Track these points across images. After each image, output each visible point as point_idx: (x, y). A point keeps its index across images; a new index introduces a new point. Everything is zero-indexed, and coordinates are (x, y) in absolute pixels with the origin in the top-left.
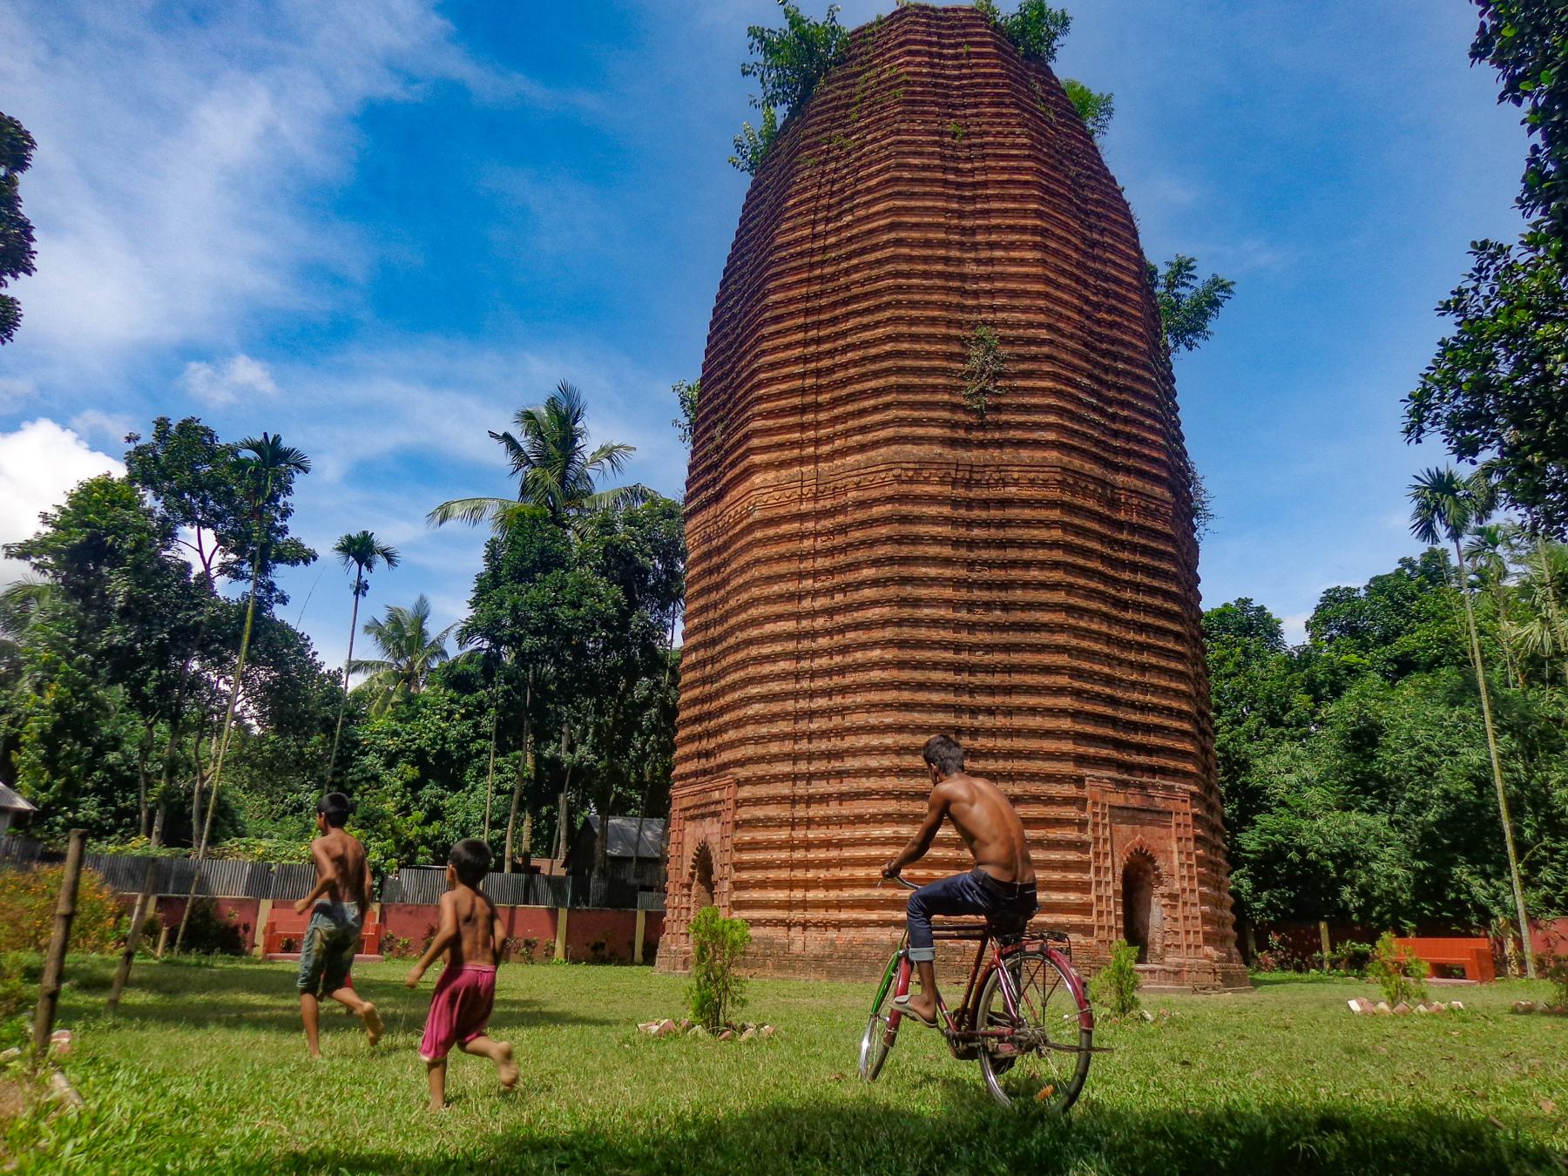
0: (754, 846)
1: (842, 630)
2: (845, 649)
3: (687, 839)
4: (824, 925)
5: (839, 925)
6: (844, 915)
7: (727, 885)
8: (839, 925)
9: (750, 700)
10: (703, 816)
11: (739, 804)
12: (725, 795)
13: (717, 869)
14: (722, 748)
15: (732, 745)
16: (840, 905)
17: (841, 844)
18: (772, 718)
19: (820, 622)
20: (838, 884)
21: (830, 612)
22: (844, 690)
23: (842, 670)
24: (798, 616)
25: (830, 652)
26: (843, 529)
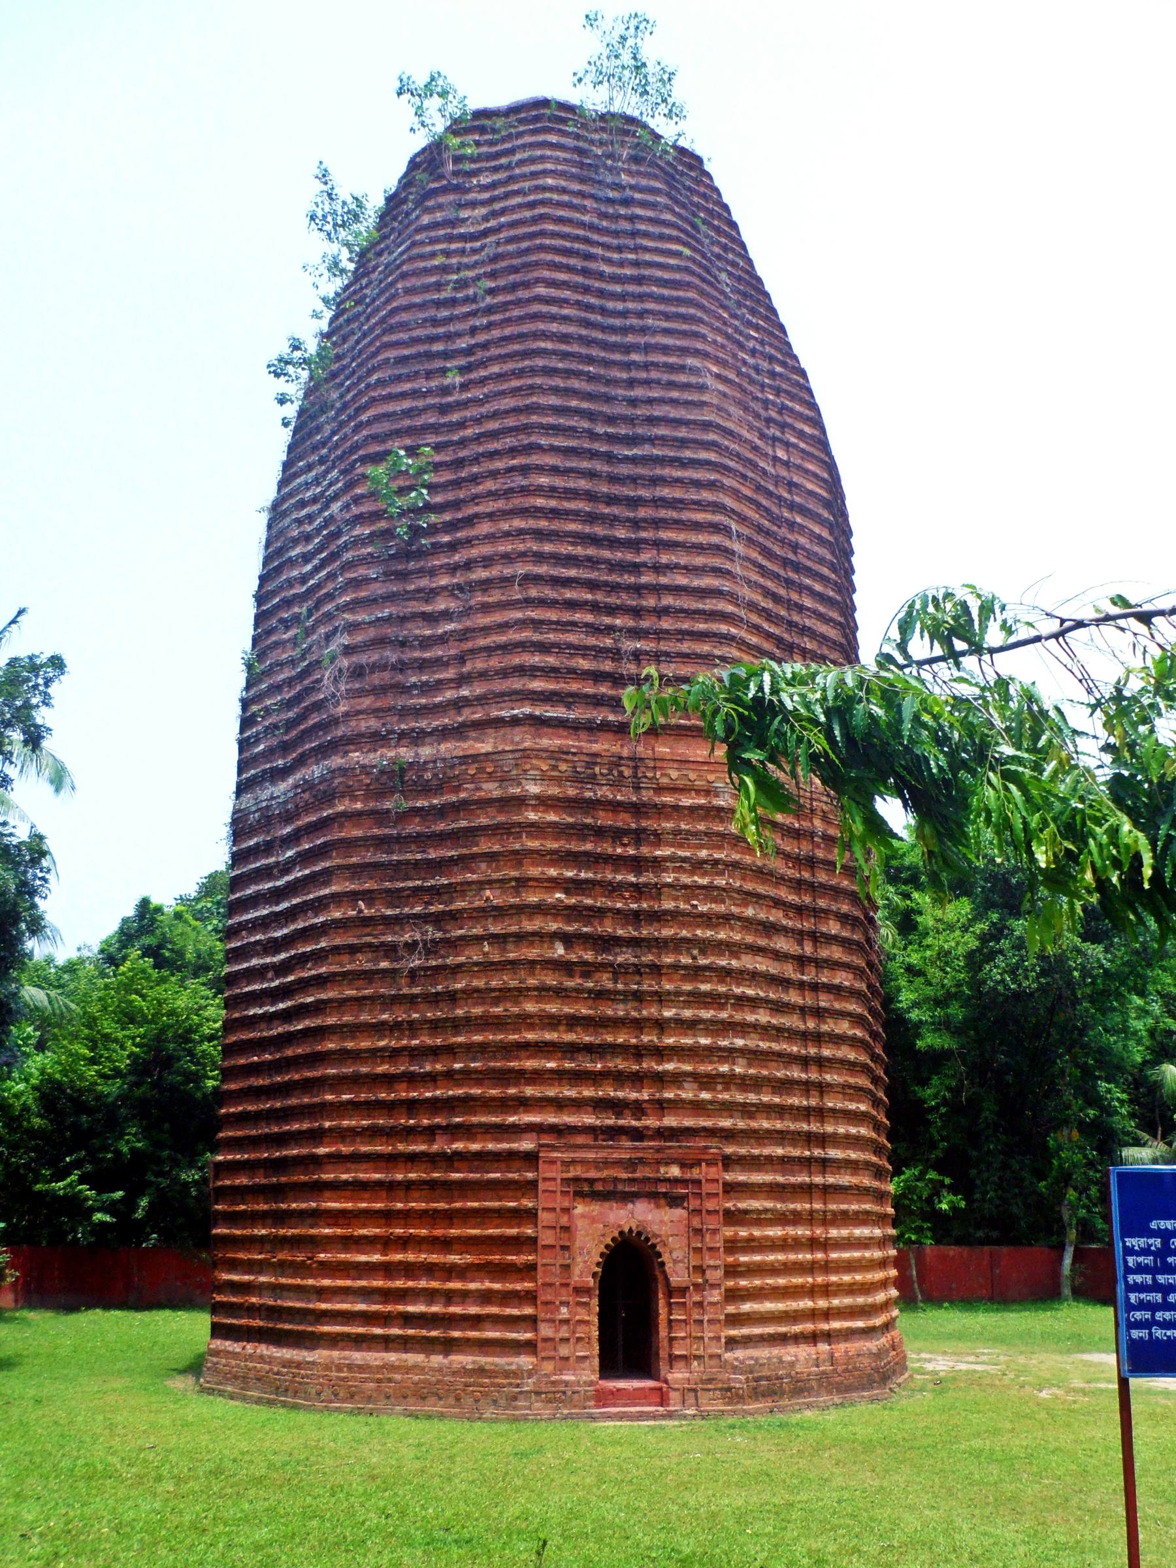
0: (751, 1245)
1: (815, 987)
2: (819, 1013)
3: (580, 1224)
4: (813, 1338)
5: (828, 1336)
6: (836, 1325)
7: (715, 1296)
8: (828, 1336)
9: (730, 1054)
10: (627, 1198)
11: (731, 1189)
12: (695, 1173)
13: (678, 1276)
14: (662, 1106)
15: (698, 1107)
16: (827, 1314)
17: (825, 1245)
18: (755, 1084)
19: (789, 971)
20: (826, 1291)
21: (801, 961)
22: (821, 1063)
23: (818, 1038)
24: (777, 956)
25: (803, 1011)
26: (811, 863)
